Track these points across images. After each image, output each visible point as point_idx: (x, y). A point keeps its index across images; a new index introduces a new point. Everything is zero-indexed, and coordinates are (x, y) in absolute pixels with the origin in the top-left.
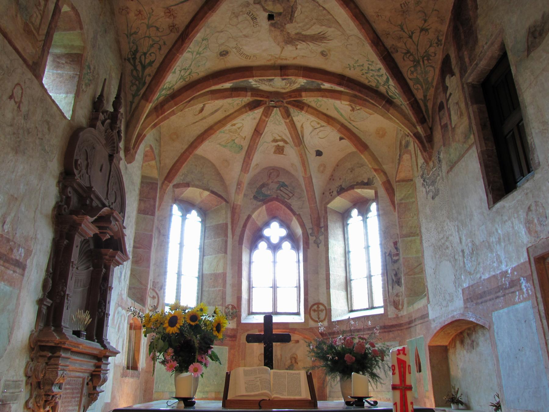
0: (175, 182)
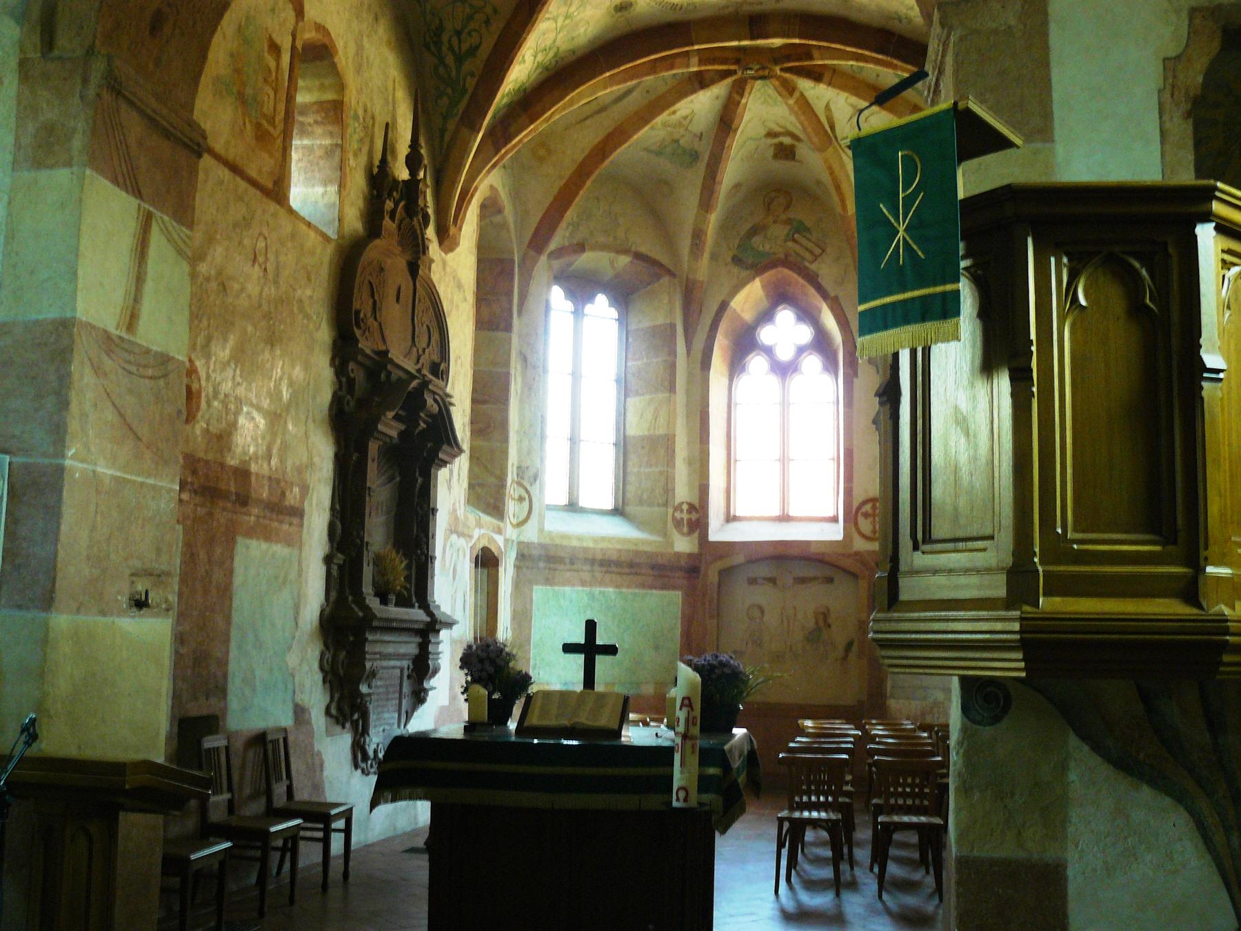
0: (553, 245)
